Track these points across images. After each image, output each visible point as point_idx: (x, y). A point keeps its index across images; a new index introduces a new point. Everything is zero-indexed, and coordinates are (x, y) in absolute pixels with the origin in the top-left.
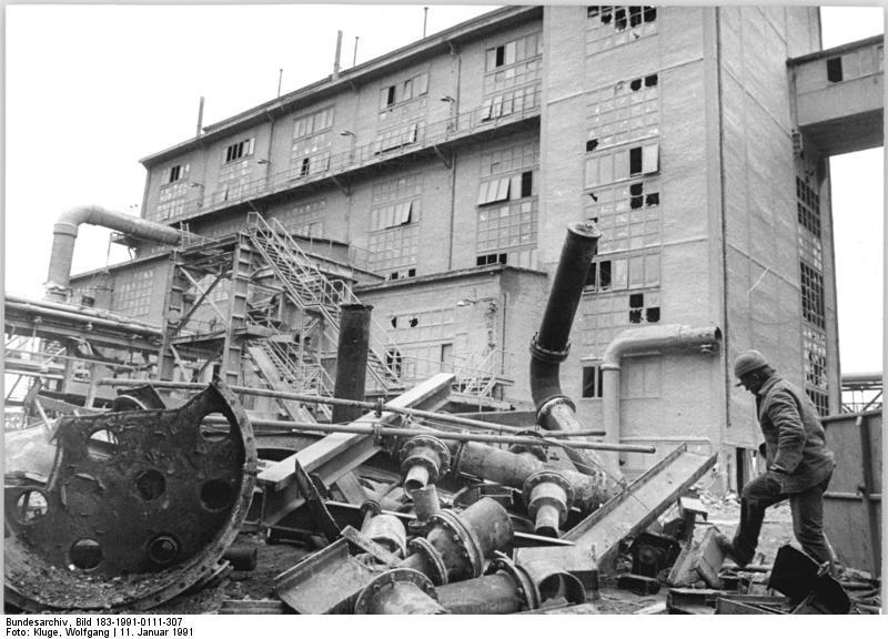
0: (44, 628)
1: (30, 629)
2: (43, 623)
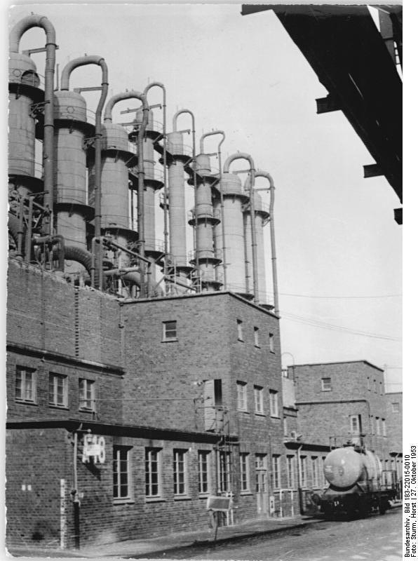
0: (411, 534)
1: (412, 541)
2: (408, 534)
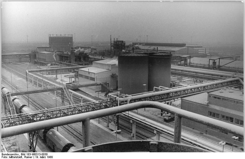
1: (8, 156)
2: (12, 155)
